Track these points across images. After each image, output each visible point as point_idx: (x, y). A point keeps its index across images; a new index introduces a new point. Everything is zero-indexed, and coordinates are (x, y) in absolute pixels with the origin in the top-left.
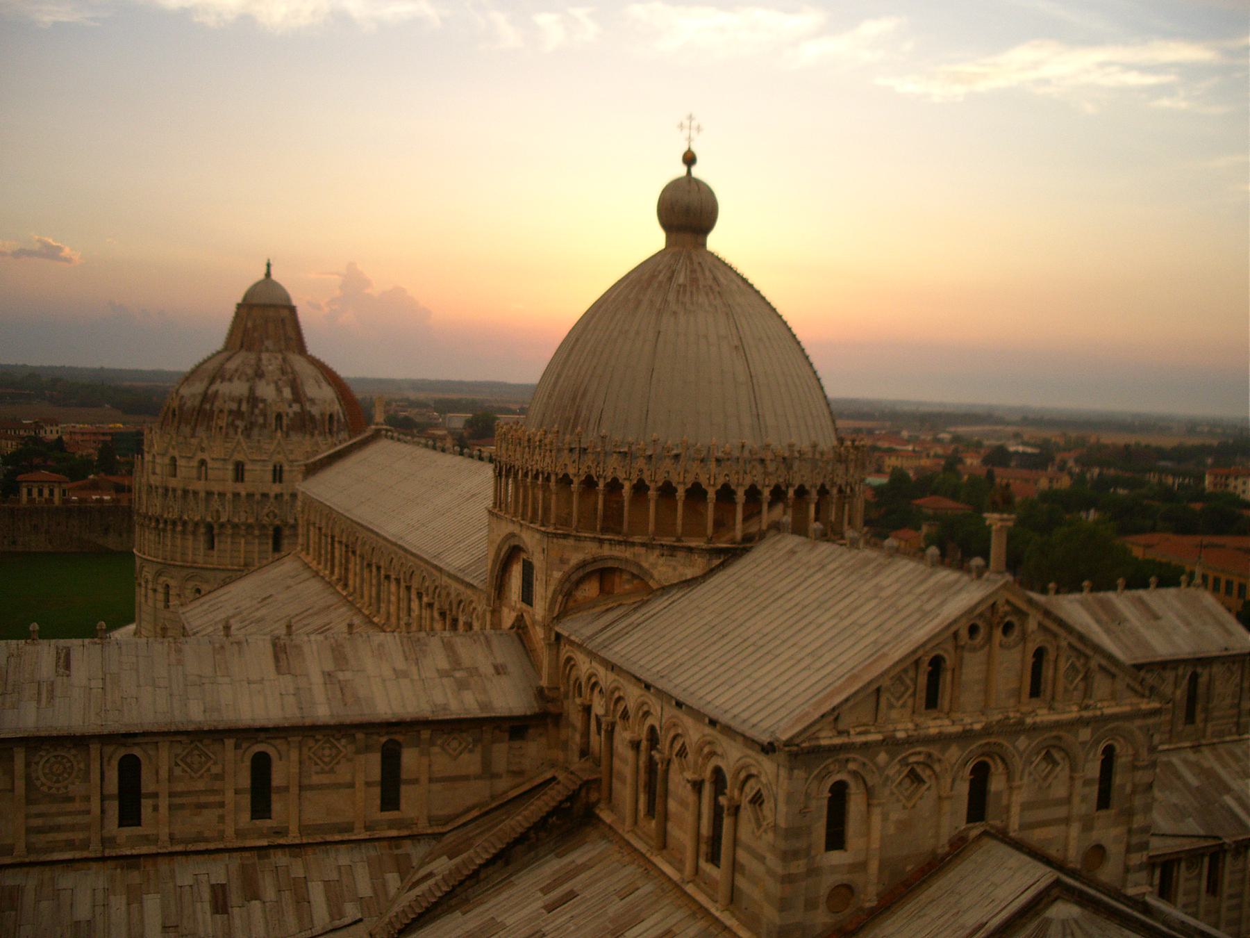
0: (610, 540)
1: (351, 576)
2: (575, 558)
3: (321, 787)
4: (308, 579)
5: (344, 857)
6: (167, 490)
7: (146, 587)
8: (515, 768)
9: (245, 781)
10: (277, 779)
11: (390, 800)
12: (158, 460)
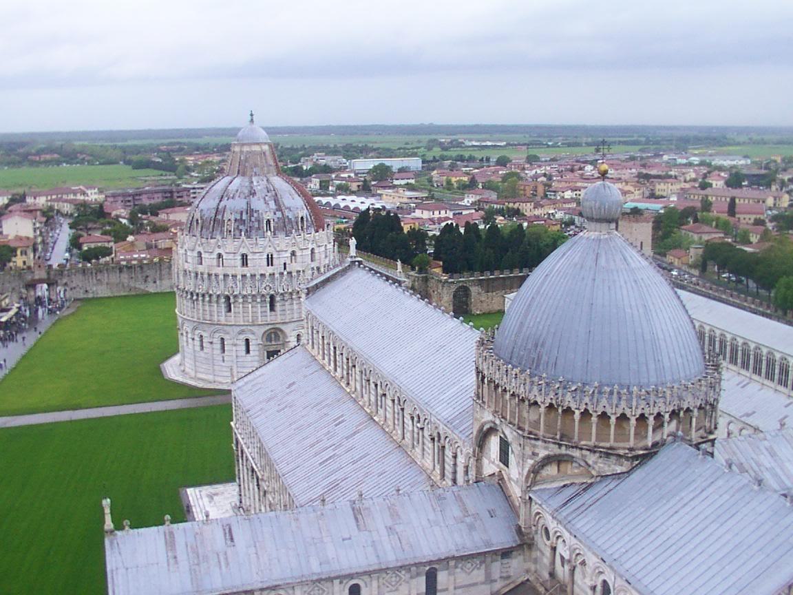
0: (566, 445)
2: (543, 453)
8: (505, 575)
12: (189, 253)
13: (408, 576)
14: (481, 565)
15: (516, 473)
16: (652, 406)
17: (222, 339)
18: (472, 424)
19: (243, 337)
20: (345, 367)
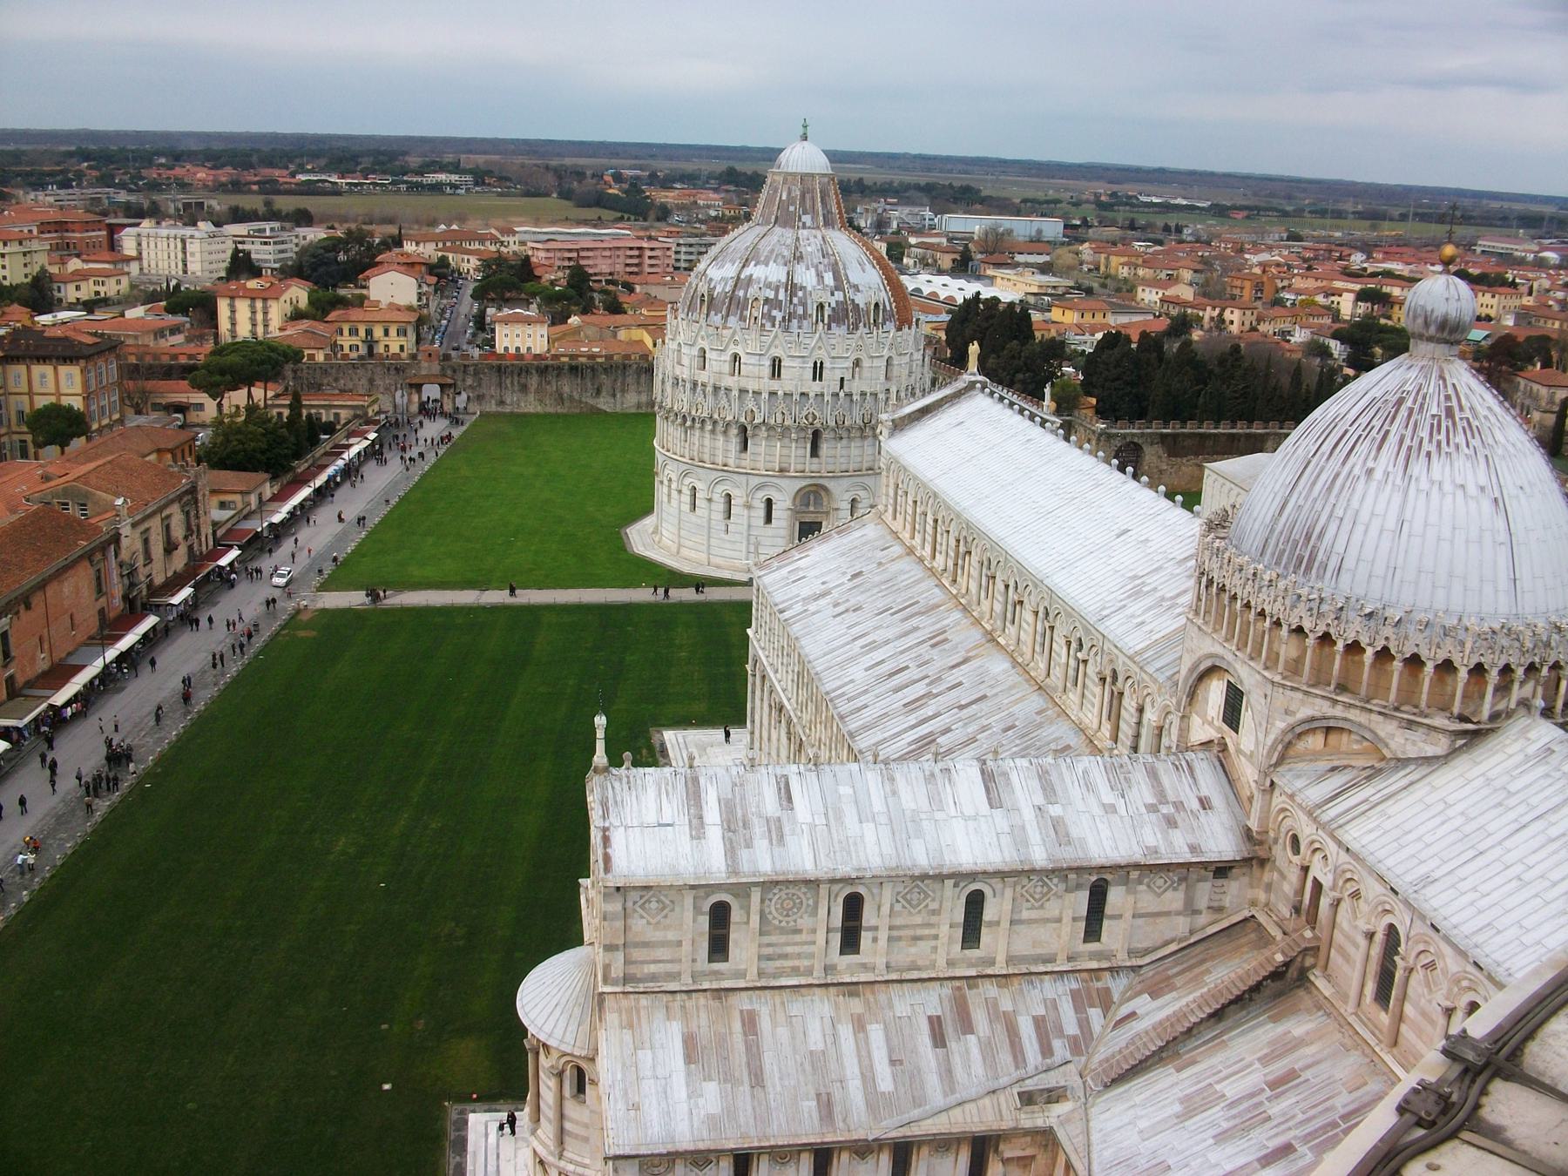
2: (1304, 712)
3: (1030, 922)
4: (900, 557)
5: (1050, 988)
6: (695, 384)
7: (670, 487)
8: (1215, 904)
9: (960, 917)
10: (989, 914)
11: (1093, 930)
12: (685, 350)
13: (1062, 886)
15: (1251, 739)
16: (1497, 653)
17: (729, 496)
18: (1181, 657)
19: (762, 495)
20: (952, 554)
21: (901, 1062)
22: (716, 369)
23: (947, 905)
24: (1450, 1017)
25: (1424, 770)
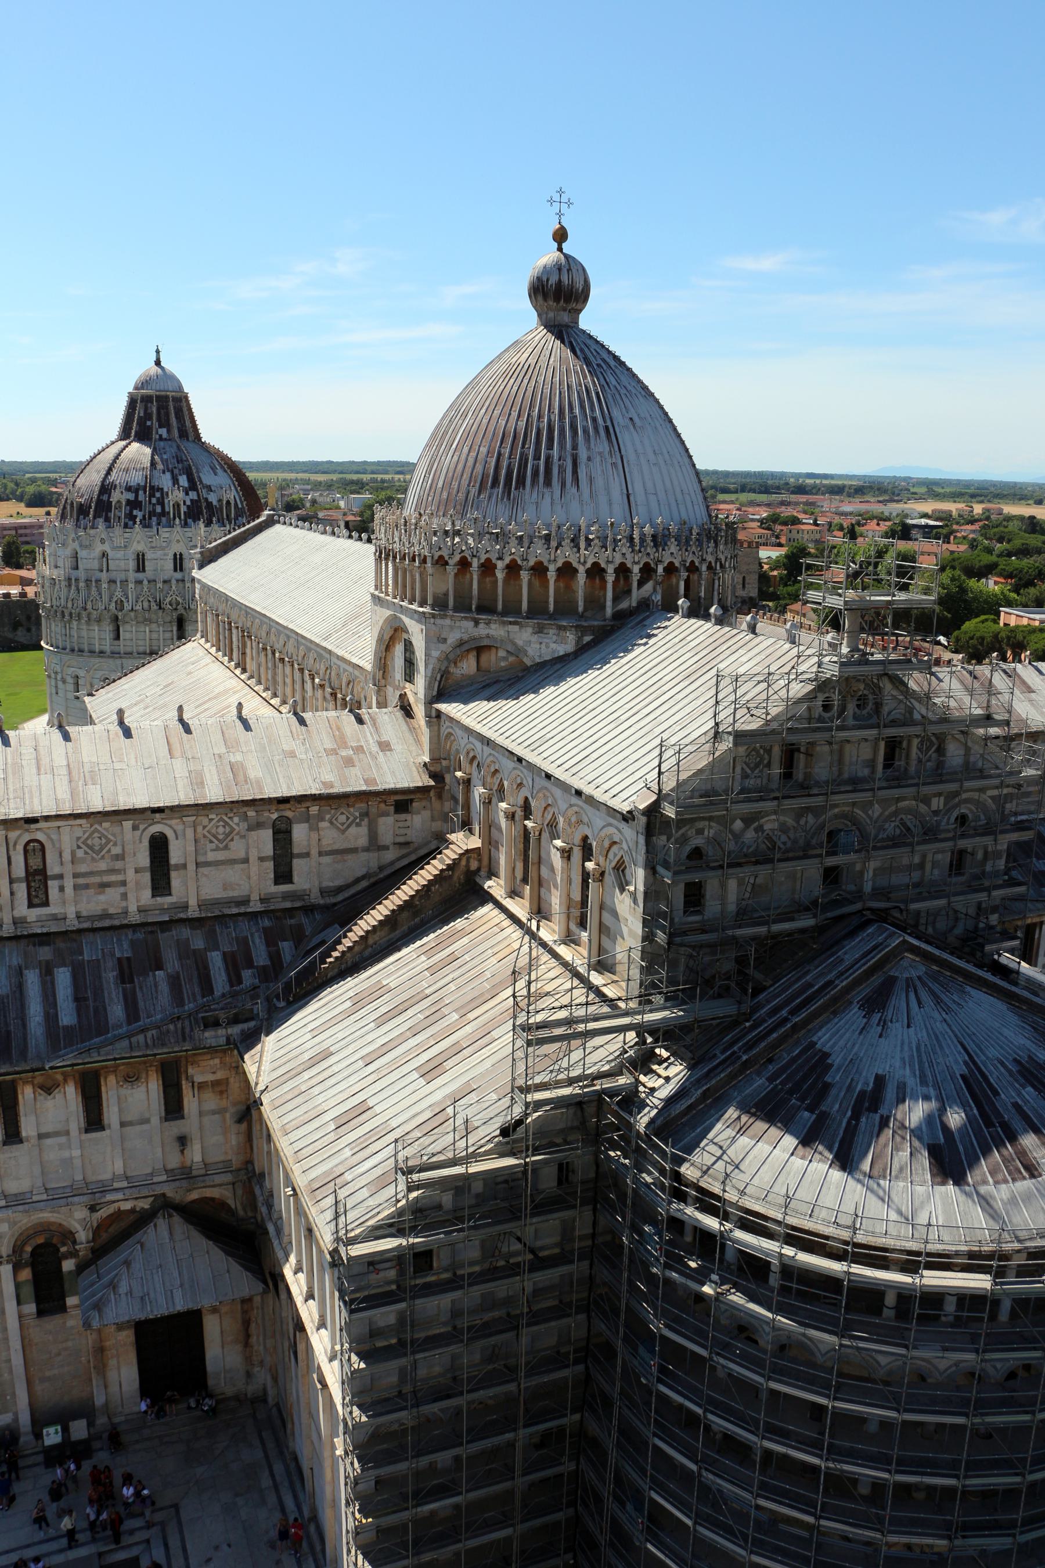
1: (248, 660)
2: (453, 638)
5: (245, 927)
8: (401, 840)
9: (144, 859)
10: (175, 857)
13: (245, 825)
14: (361, 820)
21: (86, 999)
22: (89, 566)
23: (129, 848)
24: (569, 858)
25: (558, 666)
